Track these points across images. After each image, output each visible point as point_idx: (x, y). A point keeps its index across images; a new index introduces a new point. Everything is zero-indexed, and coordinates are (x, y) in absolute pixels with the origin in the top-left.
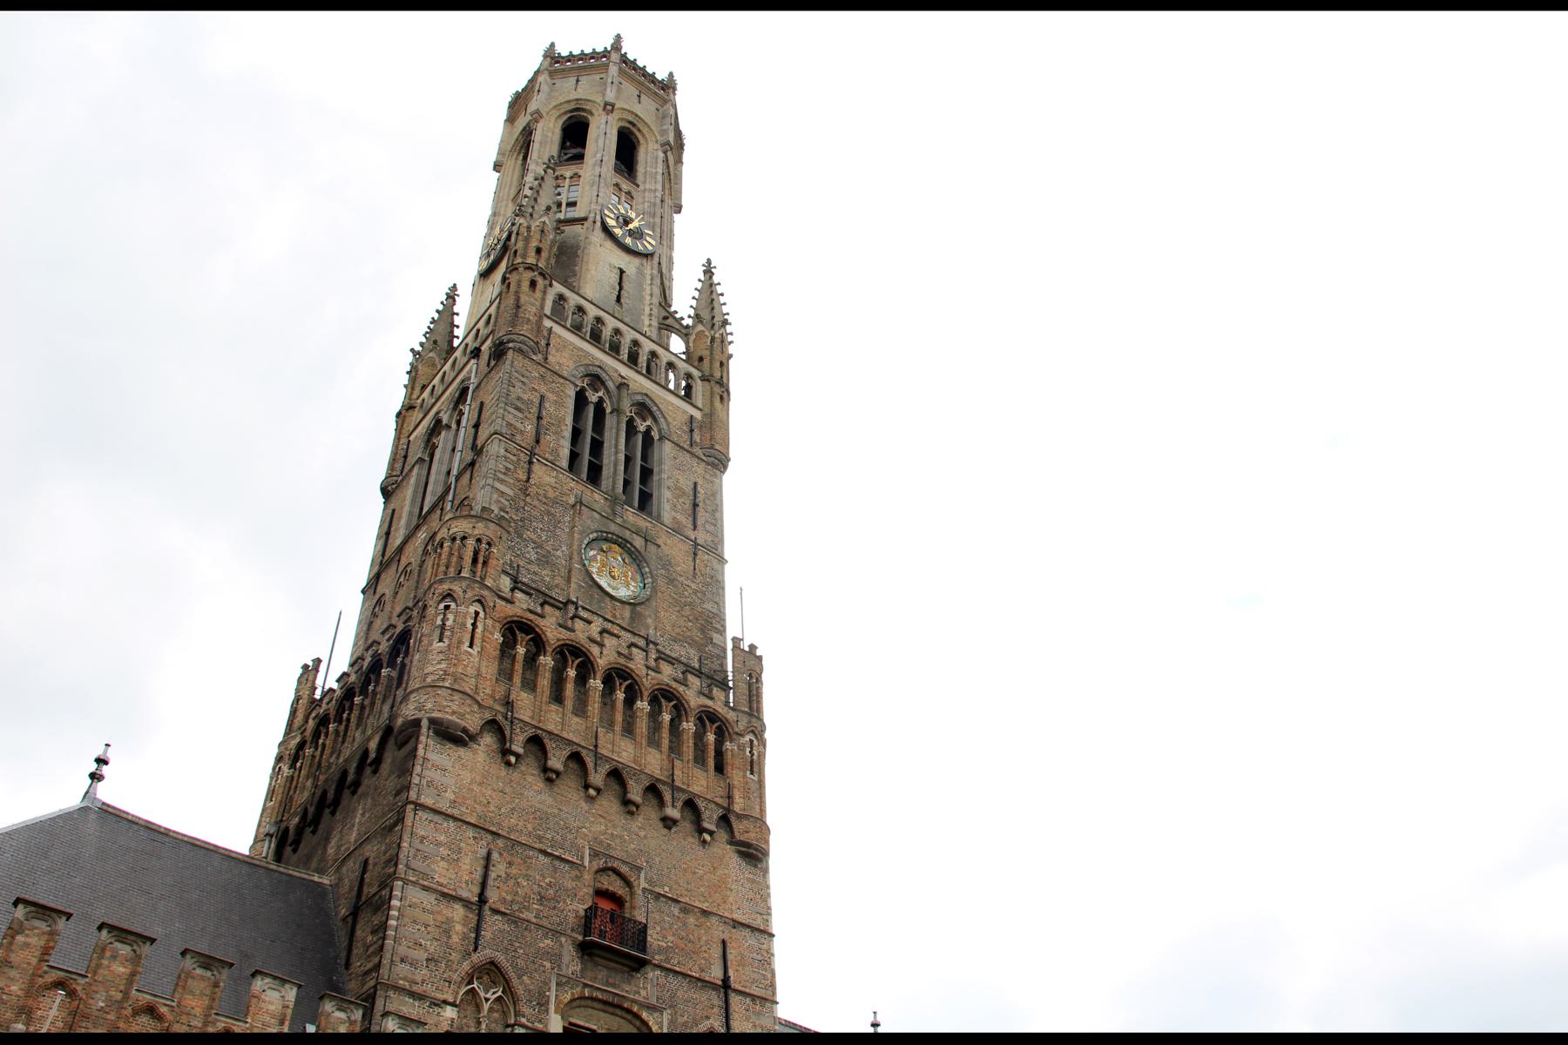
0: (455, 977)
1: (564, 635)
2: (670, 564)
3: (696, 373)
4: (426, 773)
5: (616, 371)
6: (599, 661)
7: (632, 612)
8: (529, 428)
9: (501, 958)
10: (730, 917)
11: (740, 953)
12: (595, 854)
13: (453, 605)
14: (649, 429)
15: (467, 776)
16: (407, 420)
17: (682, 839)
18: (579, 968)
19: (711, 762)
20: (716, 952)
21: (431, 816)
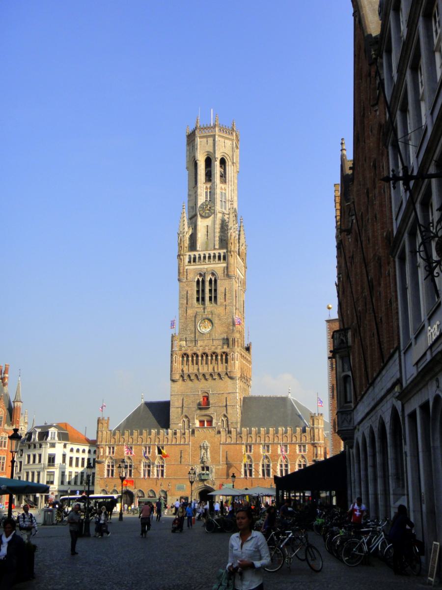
1: (192, 352)
2: (219, 315)
3: (225, 251)
5: (204, 268)
8: (185, 301)
9: (186, 414)
12: (201, 391)
14: (215, 278)
15: (179, 386)
20: (225, 401)
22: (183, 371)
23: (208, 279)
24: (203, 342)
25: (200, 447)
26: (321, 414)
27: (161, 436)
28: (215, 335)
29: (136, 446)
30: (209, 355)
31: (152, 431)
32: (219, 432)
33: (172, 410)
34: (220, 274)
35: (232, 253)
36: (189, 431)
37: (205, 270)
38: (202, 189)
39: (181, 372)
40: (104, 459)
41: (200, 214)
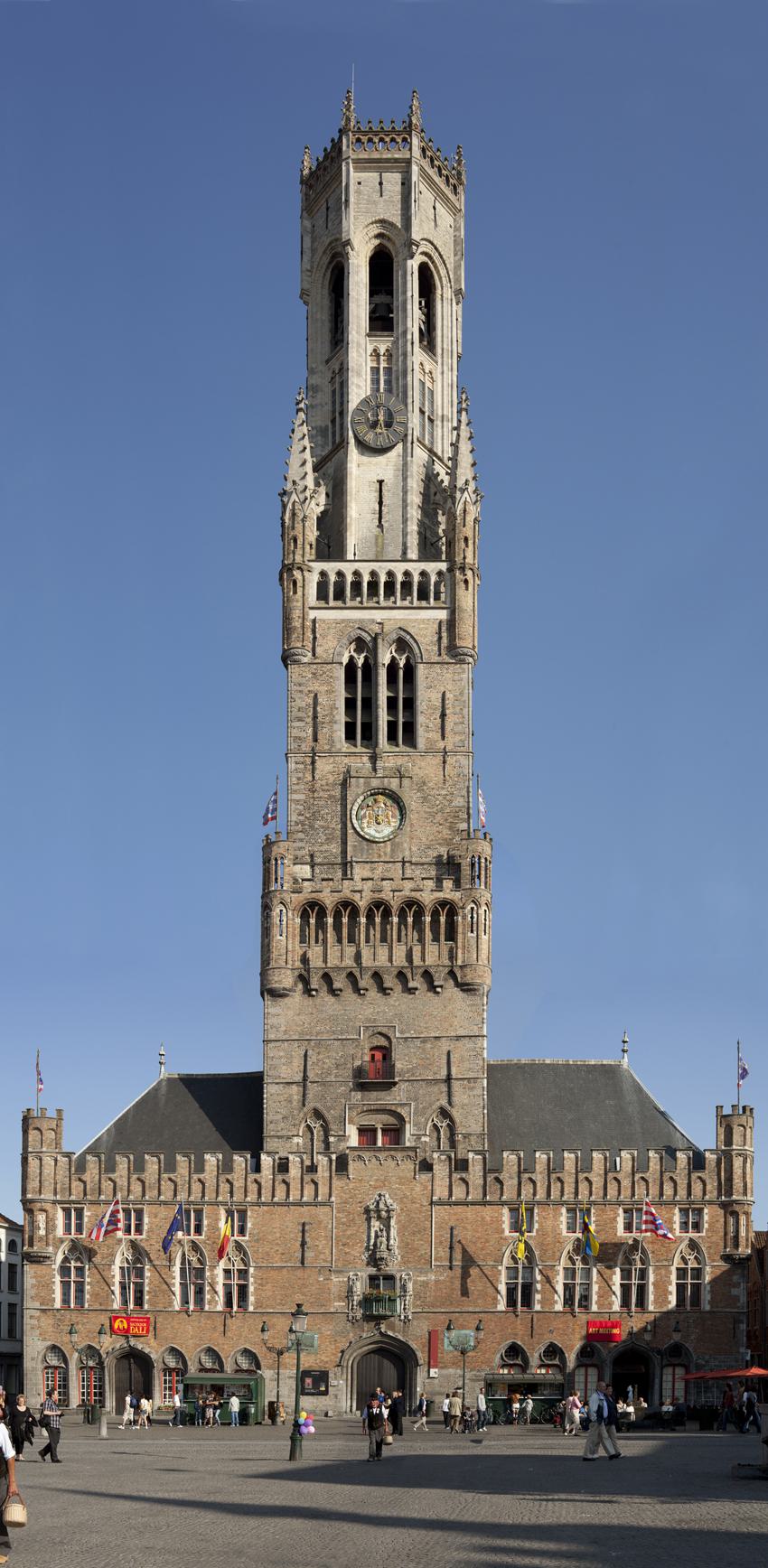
0: (297, 1122)
3: (443, 566)
4: (269, 1021)
5: (373, 621)
8: (310, 731)
9: (319, 1106)
10: (455, 1035)
11: (462, 1057)
15: (290, 1013)
19: (442, 937)
21: (273, 1044)
23: (385, 657)
24: (372, 870)
25: (367, 1211)
27: (238, 1176)
28: (410, 849)
29: (154, 1208)
31: (207, 1157)
32: (426, 1166)
33: (270, 1091)
34: (426, 640)
35: (469, 573)
36: (331, 1160)
37: (377, 629)
38: (362, 352)
39: (298, 964)
40: (51, 1249)
41: (356, 437)
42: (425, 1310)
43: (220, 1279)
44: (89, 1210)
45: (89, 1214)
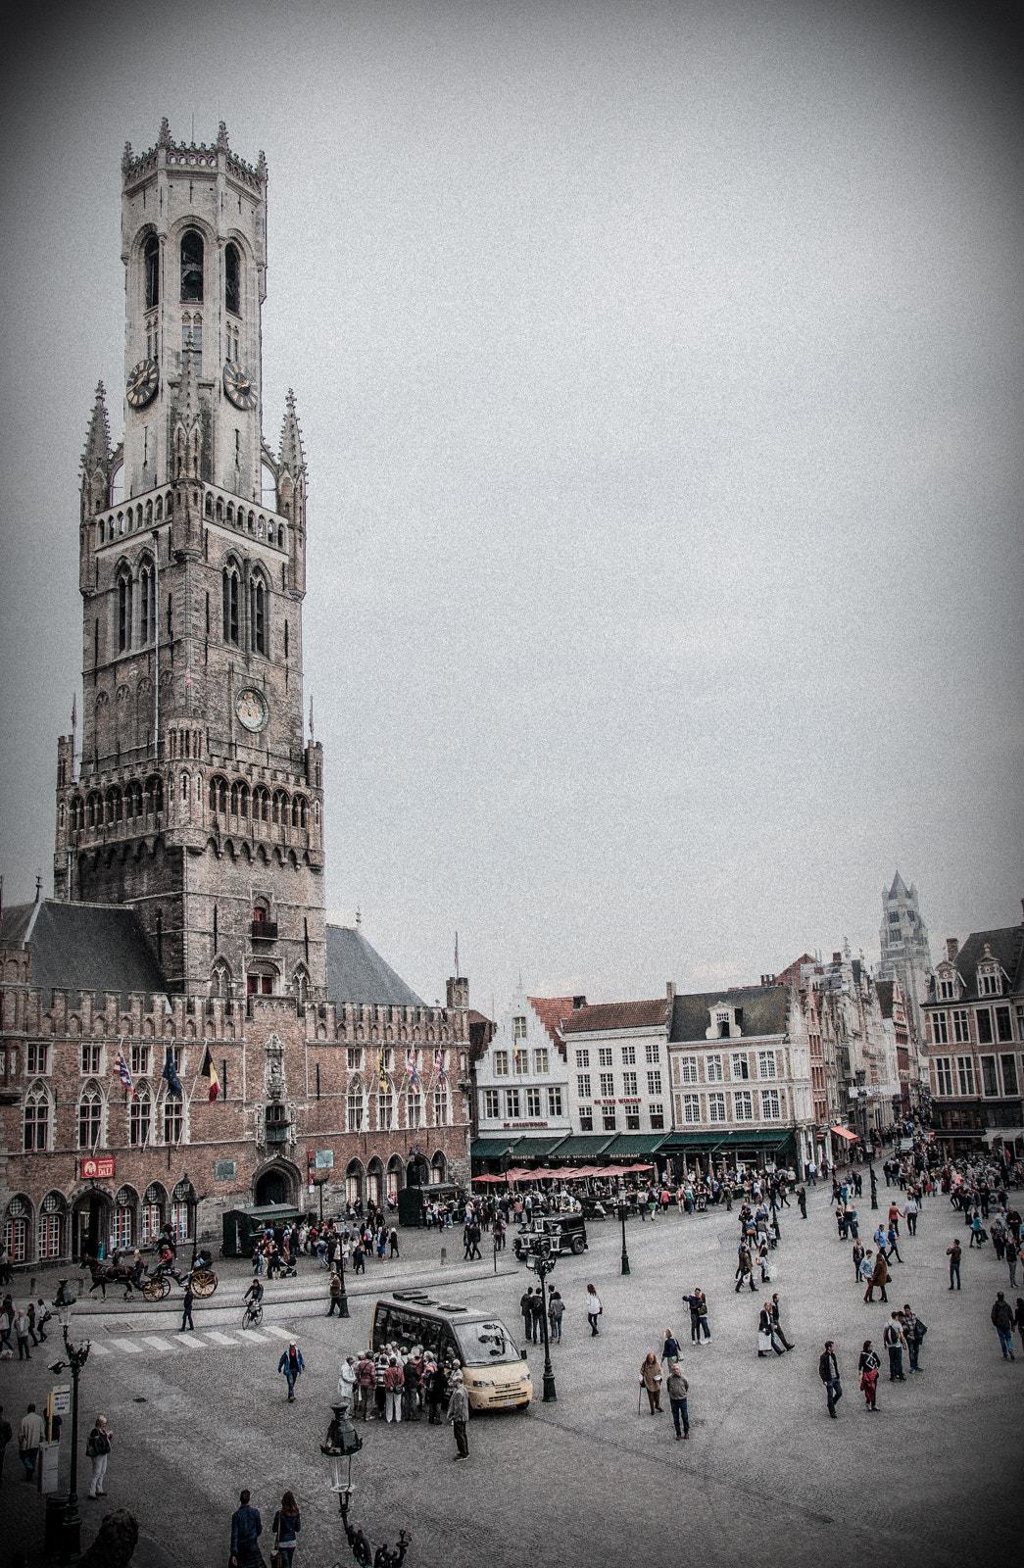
1: (236, 775)
3: (285, 522)
6: (251, 785)
7: (260, 736)
8: (203, 625)
12: (254, 892)
13: (188, 777)
14: (260, 583)
16: (92, 534)
17: (289, 872)
18: (251, 950)
19: (300, 823)
20: (303, 924)
22: (216, 826)
26: (466, 980)
30: (271, 795)
31: (155, 997)
34: (274, 571)
40: (19, 1088)
42: (305, 1135)
43: (163, 1115)
44: (55, 1047)
45: (55, 1051)
